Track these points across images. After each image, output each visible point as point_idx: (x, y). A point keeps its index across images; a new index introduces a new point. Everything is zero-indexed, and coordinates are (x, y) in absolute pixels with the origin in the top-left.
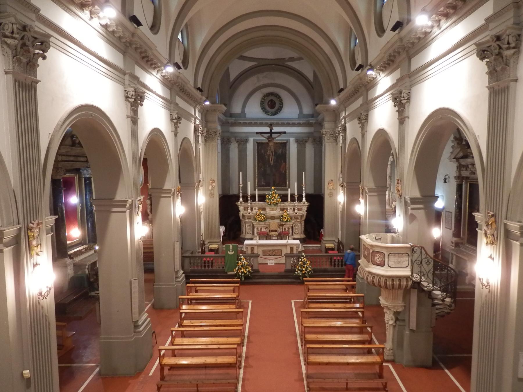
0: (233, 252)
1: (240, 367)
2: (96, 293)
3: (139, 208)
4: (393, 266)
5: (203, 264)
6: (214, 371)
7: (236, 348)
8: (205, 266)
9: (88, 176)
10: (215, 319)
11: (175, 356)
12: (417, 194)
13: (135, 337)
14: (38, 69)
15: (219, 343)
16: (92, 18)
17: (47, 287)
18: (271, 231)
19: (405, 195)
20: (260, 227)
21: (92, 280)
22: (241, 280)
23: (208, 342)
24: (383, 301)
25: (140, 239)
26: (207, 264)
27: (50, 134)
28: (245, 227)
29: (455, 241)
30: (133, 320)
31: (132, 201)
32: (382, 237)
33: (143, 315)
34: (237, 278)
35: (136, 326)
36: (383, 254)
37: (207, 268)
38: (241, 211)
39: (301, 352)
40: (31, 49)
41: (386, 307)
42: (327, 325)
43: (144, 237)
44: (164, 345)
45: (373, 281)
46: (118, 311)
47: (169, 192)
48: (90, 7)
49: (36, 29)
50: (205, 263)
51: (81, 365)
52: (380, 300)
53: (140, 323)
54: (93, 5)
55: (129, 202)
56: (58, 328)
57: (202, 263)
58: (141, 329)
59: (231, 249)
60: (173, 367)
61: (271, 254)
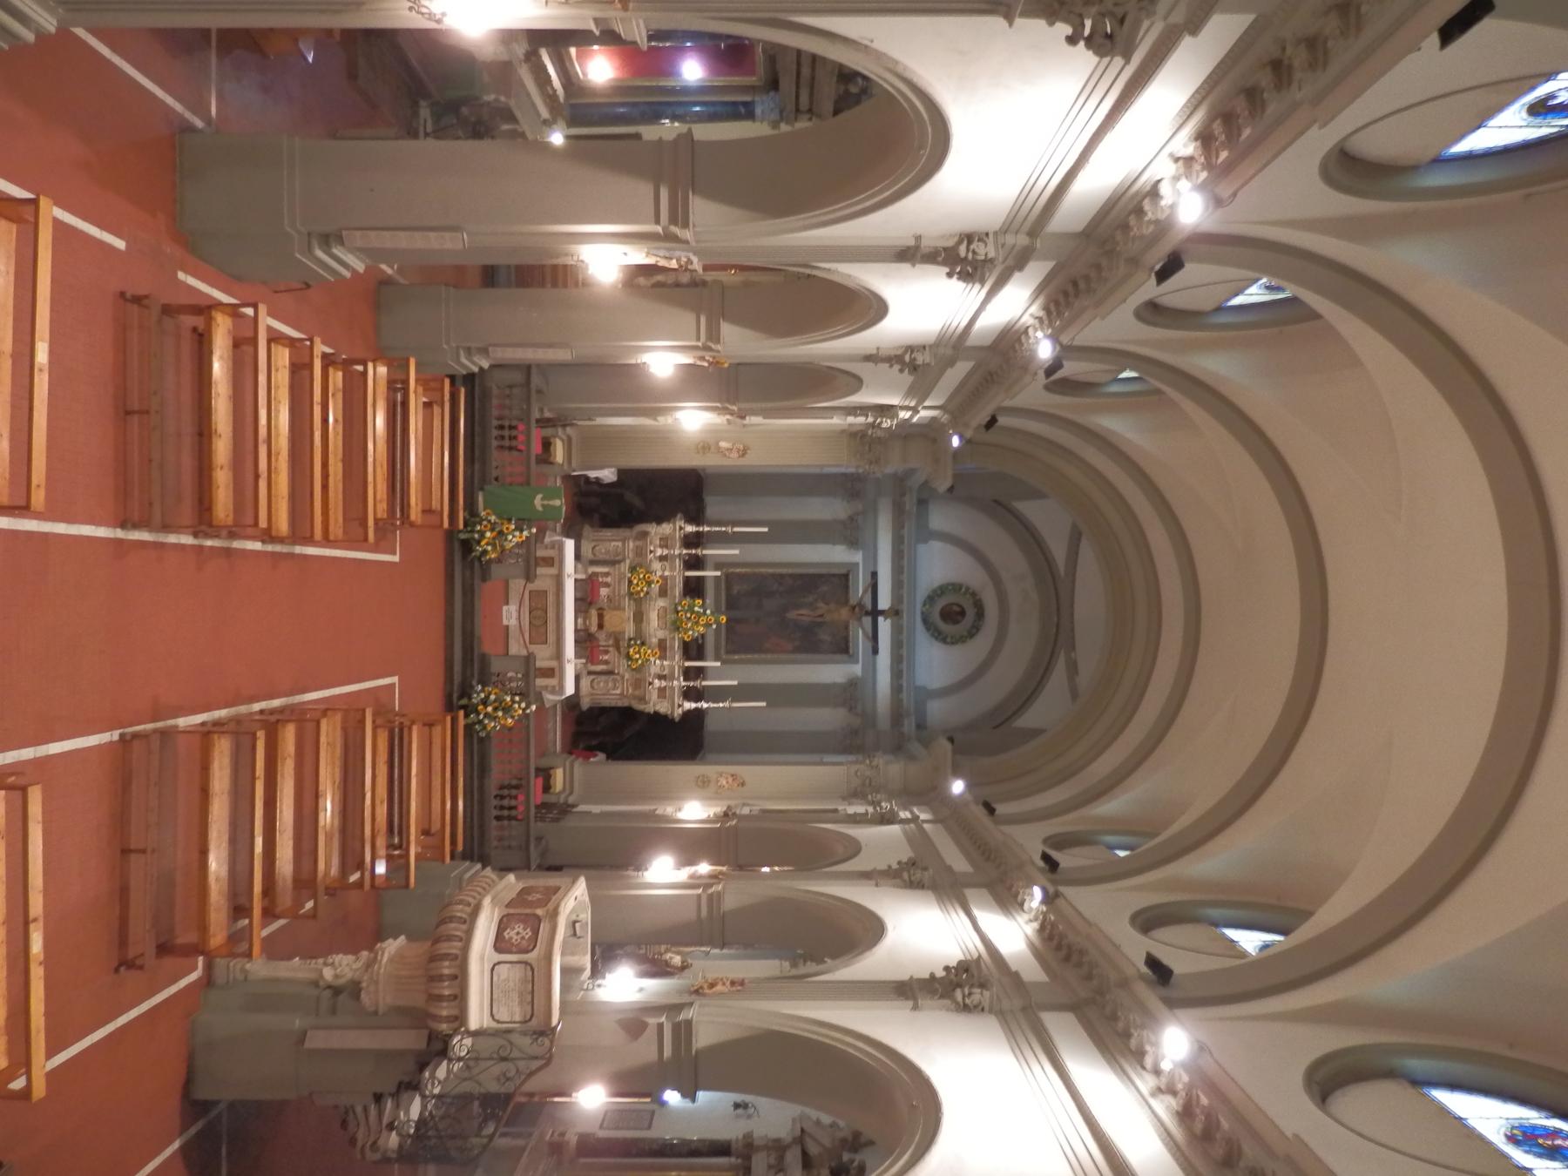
0: (540, 509)
1: (201, 535)
2: (425, 121)
3: (666, 258)
4: (495, 978)
5: (506, 423)
6: (188, 461)
7: (256, 524)
8: (501, 427)
9: (758, 111)
10: (344, 461)
11: (237, 344)
12: (703, 1038)
13: (293, 232)
14: (1040, 23)
15: (273, 476)
16: (1177, 160)
17: (444, 14)
18: (600, 612)
19: (700, 1006)
20: (613, 583)
21: (465, 110)
22: (460, 531)
23: (277, 441)
24: (392, 947)
25: (581, 258)
26: (506, 433)
27: (872, 41)
28: (614, 540)
29: (568, 1143)
30: (344, 233)
31: (687, 242)
32: (581, 940)
33: (358, 258)
34: (464, 518)
35: (327, 240)
36: (531, 947)
37: (495, 433)
38: (659, 527)
39: (243, 709)
40: (1094, 10)
41: (376, 958)
42: (321, 788)
43: (587, 268)
44: (271, 314)
45: (451, 919)
46: (372, 190)
47: (714, 335)
48: (1202, 159)
49: (1146, 24)
50: (511, 428)
51: (214, 75)
52: (395, 938)
53: (337, 251)
54: (1209, 166)
55: (686, 234)
56: (329, 32)
57: (511, 420)
58: (320, 254)
59: (551, 503)
60: (202, 340)
61: (534, 613)
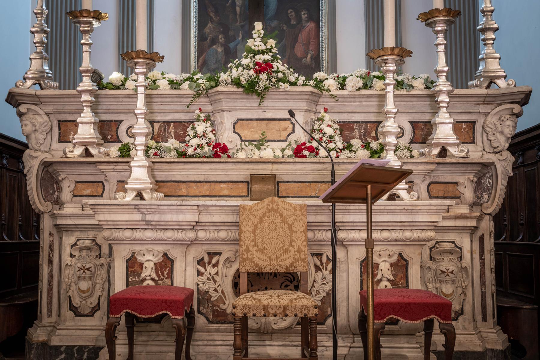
18: (244, 282)
